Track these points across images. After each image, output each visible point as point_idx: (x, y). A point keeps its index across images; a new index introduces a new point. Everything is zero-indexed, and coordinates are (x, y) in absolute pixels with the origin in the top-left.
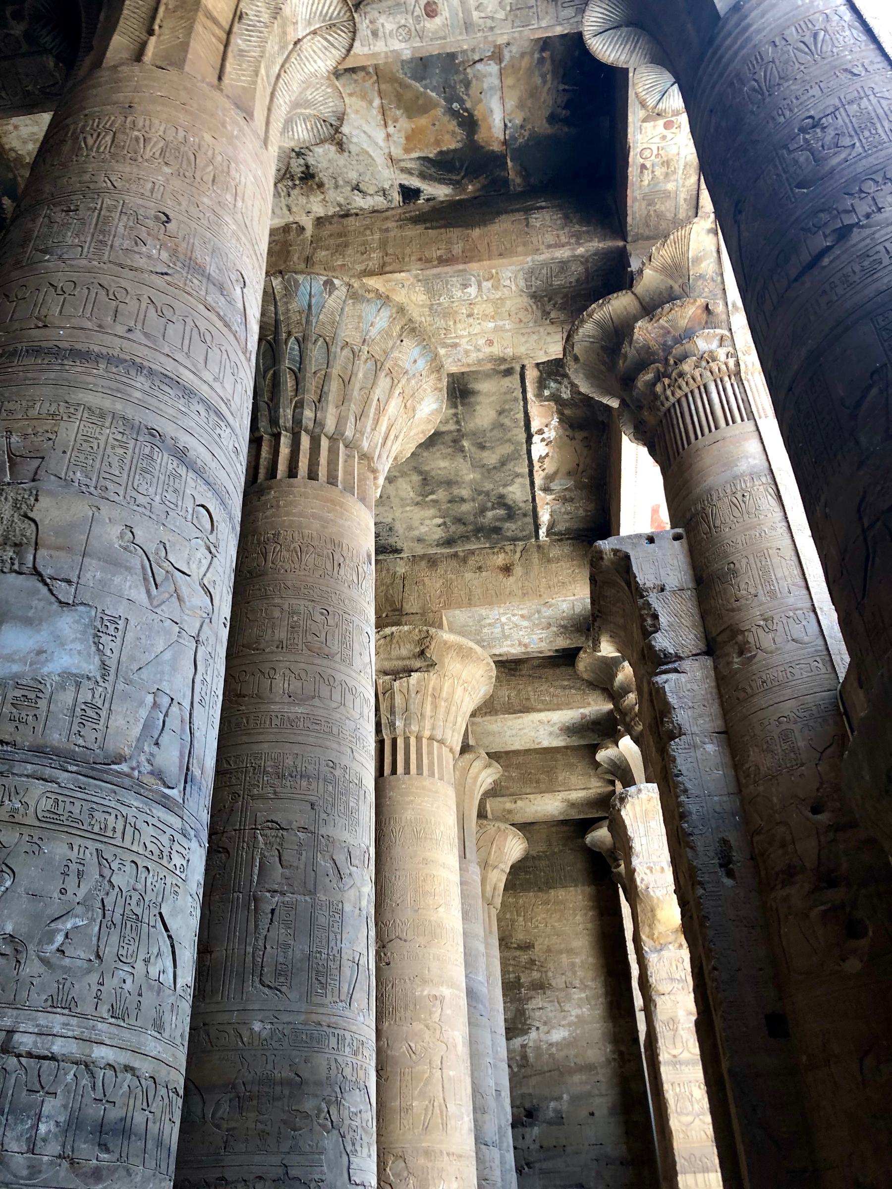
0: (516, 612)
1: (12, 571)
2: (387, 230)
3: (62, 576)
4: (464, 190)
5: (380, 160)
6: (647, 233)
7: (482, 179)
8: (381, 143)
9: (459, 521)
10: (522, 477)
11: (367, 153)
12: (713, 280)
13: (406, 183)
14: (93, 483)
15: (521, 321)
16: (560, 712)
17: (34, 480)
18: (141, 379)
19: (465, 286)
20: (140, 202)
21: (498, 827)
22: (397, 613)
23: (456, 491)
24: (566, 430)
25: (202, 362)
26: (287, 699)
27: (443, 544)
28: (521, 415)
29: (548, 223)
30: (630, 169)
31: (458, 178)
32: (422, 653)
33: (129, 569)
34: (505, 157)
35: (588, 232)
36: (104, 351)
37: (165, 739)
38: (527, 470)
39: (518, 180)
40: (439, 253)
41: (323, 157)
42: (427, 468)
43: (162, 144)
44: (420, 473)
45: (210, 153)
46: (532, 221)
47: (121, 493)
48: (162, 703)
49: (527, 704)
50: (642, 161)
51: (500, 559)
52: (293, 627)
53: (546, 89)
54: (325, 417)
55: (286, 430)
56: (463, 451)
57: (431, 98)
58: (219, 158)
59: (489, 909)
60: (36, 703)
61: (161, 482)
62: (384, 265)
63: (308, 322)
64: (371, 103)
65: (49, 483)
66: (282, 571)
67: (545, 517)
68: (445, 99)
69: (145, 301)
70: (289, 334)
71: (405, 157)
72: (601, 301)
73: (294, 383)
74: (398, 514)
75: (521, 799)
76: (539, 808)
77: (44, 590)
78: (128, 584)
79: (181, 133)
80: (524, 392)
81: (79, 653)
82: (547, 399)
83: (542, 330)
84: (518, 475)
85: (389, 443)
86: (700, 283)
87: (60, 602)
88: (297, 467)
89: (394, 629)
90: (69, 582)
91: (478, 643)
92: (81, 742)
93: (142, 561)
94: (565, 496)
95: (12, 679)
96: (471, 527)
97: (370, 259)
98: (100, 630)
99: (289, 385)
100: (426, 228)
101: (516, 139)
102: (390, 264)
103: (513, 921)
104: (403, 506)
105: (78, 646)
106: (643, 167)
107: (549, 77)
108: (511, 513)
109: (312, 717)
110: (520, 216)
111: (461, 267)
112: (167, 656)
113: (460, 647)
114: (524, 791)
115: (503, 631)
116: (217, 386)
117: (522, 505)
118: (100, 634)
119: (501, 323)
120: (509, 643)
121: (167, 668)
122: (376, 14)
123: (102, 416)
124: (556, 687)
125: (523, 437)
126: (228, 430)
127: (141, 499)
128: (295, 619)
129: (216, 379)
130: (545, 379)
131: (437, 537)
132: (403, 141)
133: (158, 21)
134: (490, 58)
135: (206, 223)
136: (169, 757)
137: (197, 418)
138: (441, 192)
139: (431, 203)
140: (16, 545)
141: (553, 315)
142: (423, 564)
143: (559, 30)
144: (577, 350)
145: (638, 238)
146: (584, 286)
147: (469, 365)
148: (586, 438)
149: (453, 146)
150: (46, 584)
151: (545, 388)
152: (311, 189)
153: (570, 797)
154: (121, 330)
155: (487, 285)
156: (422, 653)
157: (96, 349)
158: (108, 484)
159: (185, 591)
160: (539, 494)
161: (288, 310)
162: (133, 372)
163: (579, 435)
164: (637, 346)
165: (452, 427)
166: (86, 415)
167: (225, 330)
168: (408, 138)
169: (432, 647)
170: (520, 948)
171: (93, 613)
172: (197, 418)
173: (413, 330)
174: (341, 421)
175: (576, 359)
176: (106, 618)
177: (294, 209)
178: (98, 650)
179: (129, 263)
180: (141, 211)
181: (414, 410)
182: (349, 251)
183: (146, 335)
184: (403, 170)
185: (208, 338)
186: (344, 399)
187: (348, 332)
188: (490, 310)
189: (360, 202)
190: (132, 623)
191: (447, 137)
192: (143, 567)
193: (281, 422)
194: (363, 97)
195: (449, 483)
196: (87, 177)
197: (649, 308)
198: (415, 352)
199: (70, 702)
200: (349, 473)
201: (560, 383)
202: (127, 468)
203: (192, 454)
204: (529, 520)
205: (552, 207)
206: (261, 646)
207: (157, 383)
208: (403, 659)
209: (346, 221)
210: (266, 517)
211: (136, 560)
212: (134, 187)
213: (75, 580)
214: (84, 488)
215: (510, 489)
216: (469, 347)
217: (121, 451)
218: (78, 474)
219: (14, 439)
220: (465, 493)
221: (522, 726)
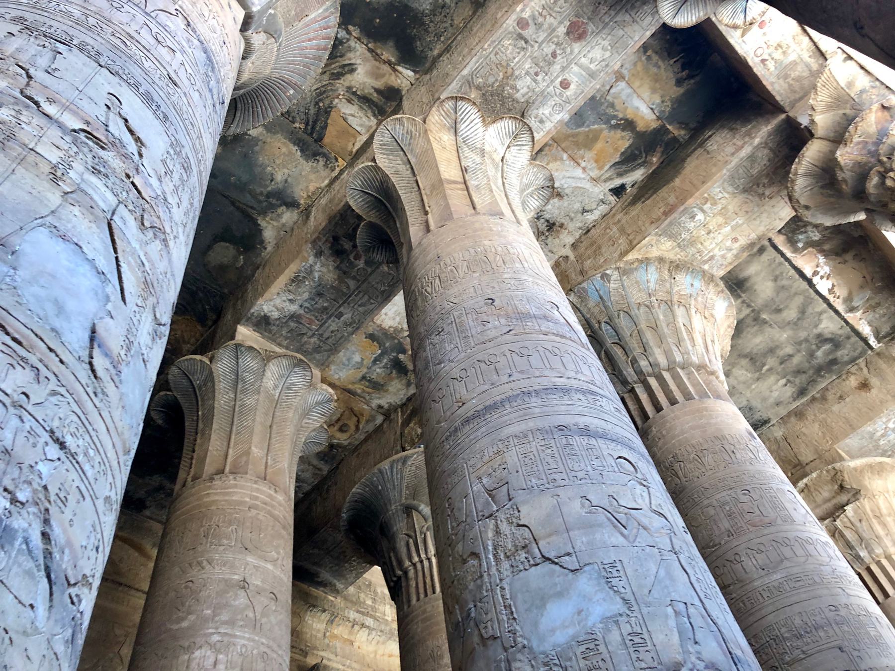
1: (531, 566)
2: (619, 221)
3: (563, 553)
4: (652, 163)
5: (588, 185)
6: (797, 96)
7: (659, 149)
8: (583, 176)
9: (799, 372)
10: (825, 312)
11: (577, 187)
12: (873, 87)
13: (612, 186)
14: (545, 481)
15: (747, 212)
17: (510, 500)
18: (534, 399)
19: (693, 217)
20: (473, 302)
22: (798, 468)
23: (781, 353)
24: (835, 260)
25: (562, 367)
26: (763, 573)
28: (792, 272)
29: (721, 141)
30: (755, 70)
31: (643, 160)
32: (842, 487)
33: (600, 525)
34: (664, 126)
35: (754, 127)
36: (503, 397)
37: (699, 636)
38: (825, 305)
39: (683, 132)
40: (662, 210)
41: (554, 209)
42: (748, 350)
43: (465, 264)
44: (745, 356)
45: (493, 250)
46: (710, 148)
47: (565, 478)
48: (682, 611)
50: (760, 58)
51: (853, 381)
52: (730, 515)
53: (663, 70)
54: (656, 359)
55: (636, 383)
56: (766, 323)
57: (596, 130)
58: (500, 249)
60: (598, 650)
61: (585, 456)
62: (631, 241)
63: (606, 307)
64: (562, 159)
65: (519, 497)
66: (696, 479)
67: (866, 330)
68: (605, 123)
69: (508, 353)
70: (599, 322)
71: (602, 172)
72: (797, 160)
73: (621, 350)
74: (748, 395)
77: (557, 567)
78: (606, 535)
79: (472, 251)
80: (783, 255)
81: (604, 600)
82: (804, 248)
83: (766, 207)
84: (821, 313)
85: (710, 348)
86: (864, 96)
87: (572, 571)
88: (658, 402)
89: (805, 480)
90: (569, 554)
91: (882, 455)
92: (643, 665)
93: (606, 516)
94: (870, 305)
95: (573, 640)
96: (811, 372)
97: (620, 245)
98: (608, 575)
99: (619, 353)
100: (643, 202)
101: (664, 111)
102: (635, 239)
104: (749, 387)
105: (600, 596)
106: (763, 61)
107: (660, 63)
108: (835, 343)
109: (791, 577)
110: (700, 151)
111: (682, 208)
112: (662, 573)
113: (871, 467)
116: (579, 376)
117: (840, 332)
118: (610, 580)
119: (734, 223)
121: (668, 582)
122: (536, 111)
123: (526, 436)
125: (805, 285)
126: (604, 400)
127: (580, 475)
128: (728, 508)
129: (577, 373)
130: (792, 237)
131: (789, 394)
132: (594, 165)
133: (426, 205)
134: (616, 81)
135: (514, 288)
136: (711, 650)
137: (581, 404)
138: (638, 175)
139: (636, 186)
140: (523, 548)
141: (767, 193)
142: (793, 419)
143: (648, 34)
144: (803, 202)
145: (793, 105)
146: (776, 160)
147: (730, 264)
148: (856, 255)
149: (627, 145)
150: (557, 564)
151: (797, 242)
152: (558, 232)
154: (505, 378)
155: (707, 207)
157: (498, 398)
158: (554, 476)
159: (645, 521)
160: (849, 316)
161: (589, 309)
162: (527, 399)
163: (849, 257)
164: (849, 168)
165: (746, 311)
166: (516, 441)
167: (563, 340)
168: (596, 161)
169: (846, 478)
171: (596, 568)
172: (581, 404)
173: (677, 266)
174: (668, 354)
175: (807, 208)
176: (606, 566)
177: (555, 250)
178: (615, 592)
179: (487, 338)
180: (476, 306)
181: (712, 316)
182: (603, 250)
183: (521, 372)
184: (605, 181)
185: (557, 351)
186: (661, 340)
187: (636, 296)
188: (720, 220)
189: (591, 218)
190: (625, 561)
191: (620, 142)
192: (609, 519)
193: (629, 380)
194: (556, 160)
195: (771, 351)
196: (438, 309)
197: (838, 138)
198: (688, 279)
199: (619, 639)
200: (696, 384)
201: (806, 232)
202: (559, 459)
203: (592, 427)
204: (855, 339)
205: (717, 130)
206: (717, 542)
207: (544, 396)
208: (829, 500)
209: (589, 234)
210: (661, 448)
211: (602, 516)
212: (465, 297)
213: (572, 551)
214: (542, 488)
215: (822, 326)
216: (723, 253)
217: (549, 451)
218: (533, 480)
219: (485, 481)
220: (789, 350)
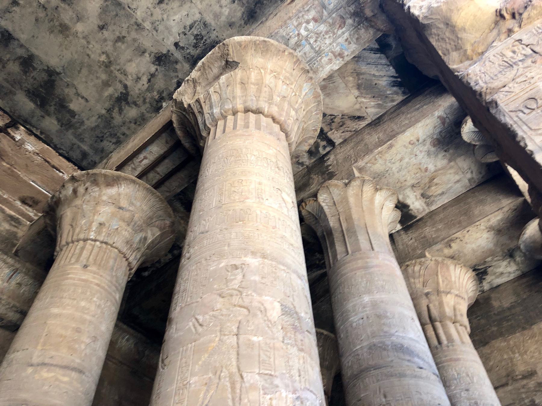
0: (306, 17)
16: (420, 125)
21: (436, 260)
27: (249, 20)
32: (227, 62)
49: (394, 133)
59: (456, 327)
75: (452, 240)
76: (474, 246)
103: (511, 359)
114: (451, 233)
115: (312, 47)
120: (325, 60)
124: (413, 112)
131: (239, 14)
153: (491, 223)
156: (227, 62)
221: (399, 157)
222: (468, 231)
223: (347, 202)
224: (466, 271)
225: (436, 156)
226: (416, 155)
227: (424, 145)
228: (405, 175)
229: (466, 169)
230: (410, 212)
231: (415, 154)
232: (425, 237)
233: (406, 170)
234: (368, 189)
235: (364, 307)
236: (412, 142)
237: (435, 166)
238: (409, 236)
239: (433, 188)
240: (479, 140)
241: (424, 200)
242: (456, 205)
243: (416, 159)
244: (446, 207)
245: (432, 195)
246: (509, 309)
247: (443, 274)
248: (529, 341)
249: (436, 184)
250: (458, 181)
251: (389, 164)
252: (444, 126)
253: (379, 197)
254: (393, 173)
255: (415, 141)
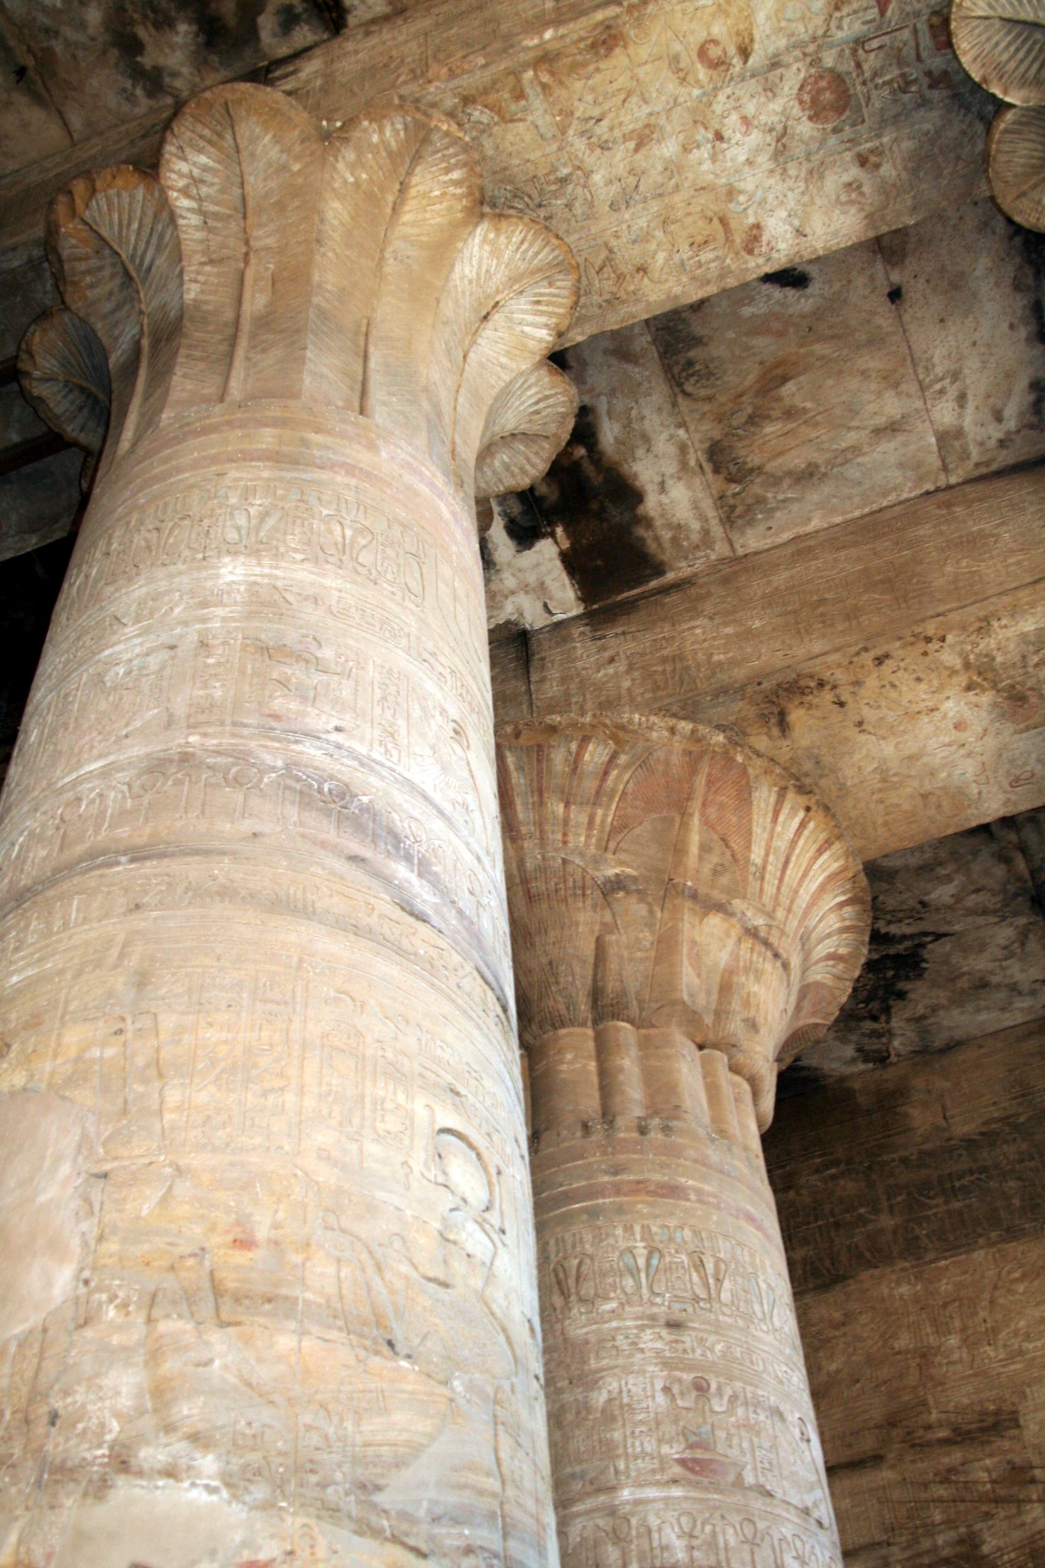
76: (888, 749)
103: (925, 1355)
170: (961, 1437)
221: (635, 115)
222: (880, 661)
223: (312, 210)
224: (823, 836)
225: (816, 174)
226: (719, 137)
227: (771, 90)
228: (645, 237)
229: (939, 370)
230: (640, 531)
231: (715, 124)
232: (678, 657)
233: (655, 207)
234: (436, 190)
235: (204, 604)
236: (714, 52)
237: (800, 233)
238: (603, 649)
239: (769, 429)
240: (1024, 82)
241: (718, 483)
242: (855, 544)
243: (714, 158)
244: (810, 549)
245: (760, 469)
246: (970, 1143)
247: (712, 812)
248: (1021, 1288)
249: (790, 414)
250: (893, 428)
251: (580, 145)
252: (882, 13)
253: (486, 256)
254: (591, 205)
255: (732, 50)
